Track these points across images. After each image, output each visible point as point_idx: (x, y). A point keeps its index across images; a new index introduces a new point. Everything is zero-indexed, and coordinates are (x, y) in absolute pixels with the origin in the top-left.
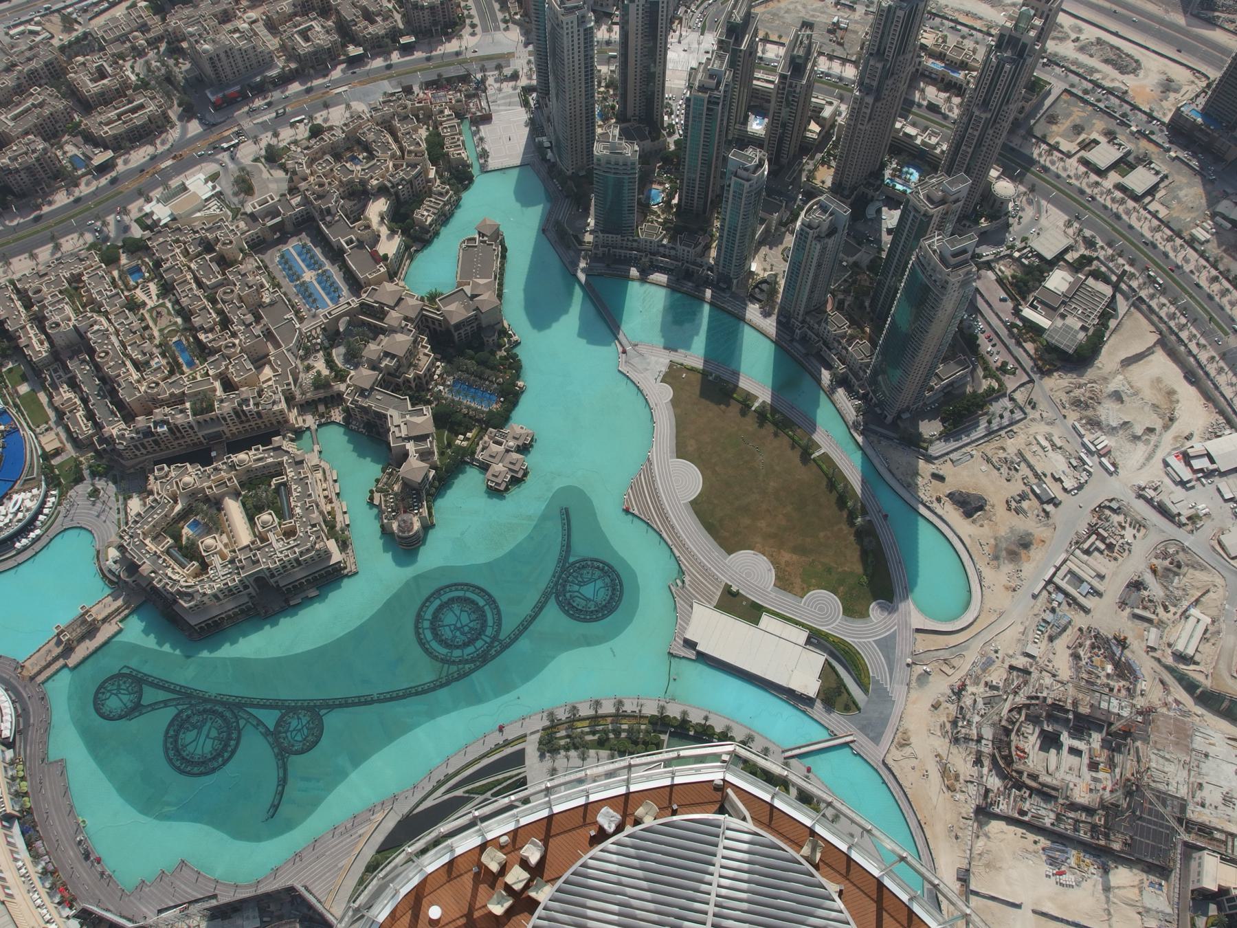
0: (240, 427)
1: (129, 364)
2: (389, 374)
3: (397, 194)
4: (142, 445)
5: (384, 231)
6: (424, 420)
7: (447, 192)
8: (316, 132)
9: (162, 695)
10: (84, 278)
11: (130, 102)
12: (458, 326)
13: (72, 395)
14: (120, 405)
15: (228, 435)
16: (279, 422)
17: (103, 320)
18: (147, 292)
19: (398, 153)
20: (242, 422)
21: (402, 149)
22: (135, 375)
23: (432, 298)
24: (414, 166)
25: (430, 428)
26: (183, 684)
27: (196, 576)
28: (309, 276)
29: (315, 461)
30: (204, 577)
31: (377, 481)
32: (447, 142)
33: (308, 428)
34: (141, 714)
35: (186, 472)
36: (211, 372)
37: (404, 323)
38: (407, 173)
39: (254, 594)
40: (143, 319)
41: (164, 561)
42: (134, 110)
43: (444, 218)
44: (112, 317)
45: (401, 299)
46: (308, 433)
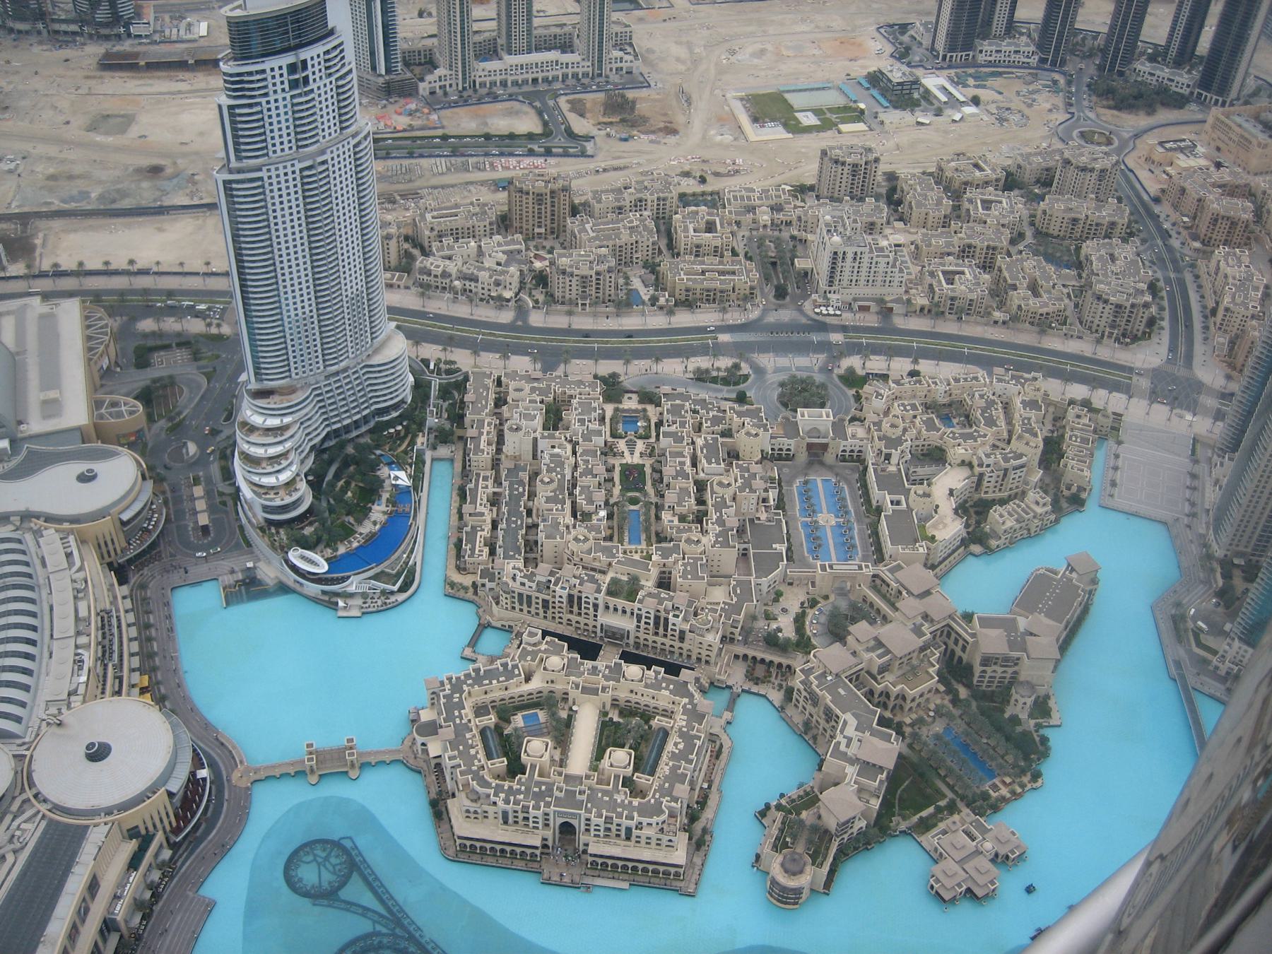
0: (651, 638)
1: (568, 505)
2: (868, 672)
3: (981, 475)
4: (529, 597)
5: (947, 507)
6: (886, 751)
7: (1044, 505)
8: (913, 374)
9: (368, 900)
10: (574, 402)
11: (721, 263)
12: (986, 661)
13: (486, 511)
14: (531, 546)
15: (631, 641)
16: (699, 660)
17: (569, 447)
18: (631, 446)
19: (1005, 435)
20: (656, 634)
21: (1010, 433)
22: (569, 520)
23: (968, 617)
24: (1020, 456)
25: (890, 764)
26: (400, 898)
27: (498, 777)
28: (827, 519)
29: (715, 730)
30: (506, 784)
31: (782, 796)
32: (1070, 453)
33: (730, 687)
34: (329, 906)
35: (558, 652)
36: (654, 558)
37: (919, 620)
38: (1006, 460)
39: (550, 843)
40: (610, 470)
41: (474, 736)
42: (722, 273)
43: (1028, 533)
44: (579, 450)
45: (927, 593)
46: (726, 695)
